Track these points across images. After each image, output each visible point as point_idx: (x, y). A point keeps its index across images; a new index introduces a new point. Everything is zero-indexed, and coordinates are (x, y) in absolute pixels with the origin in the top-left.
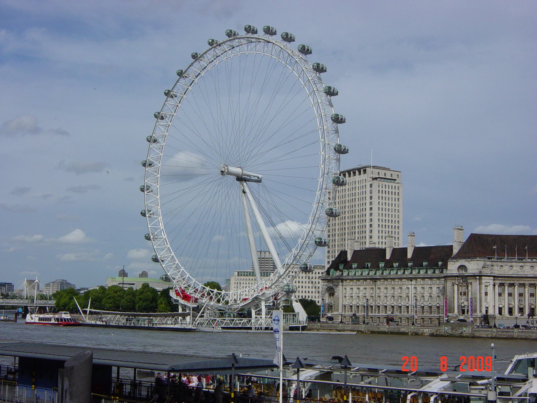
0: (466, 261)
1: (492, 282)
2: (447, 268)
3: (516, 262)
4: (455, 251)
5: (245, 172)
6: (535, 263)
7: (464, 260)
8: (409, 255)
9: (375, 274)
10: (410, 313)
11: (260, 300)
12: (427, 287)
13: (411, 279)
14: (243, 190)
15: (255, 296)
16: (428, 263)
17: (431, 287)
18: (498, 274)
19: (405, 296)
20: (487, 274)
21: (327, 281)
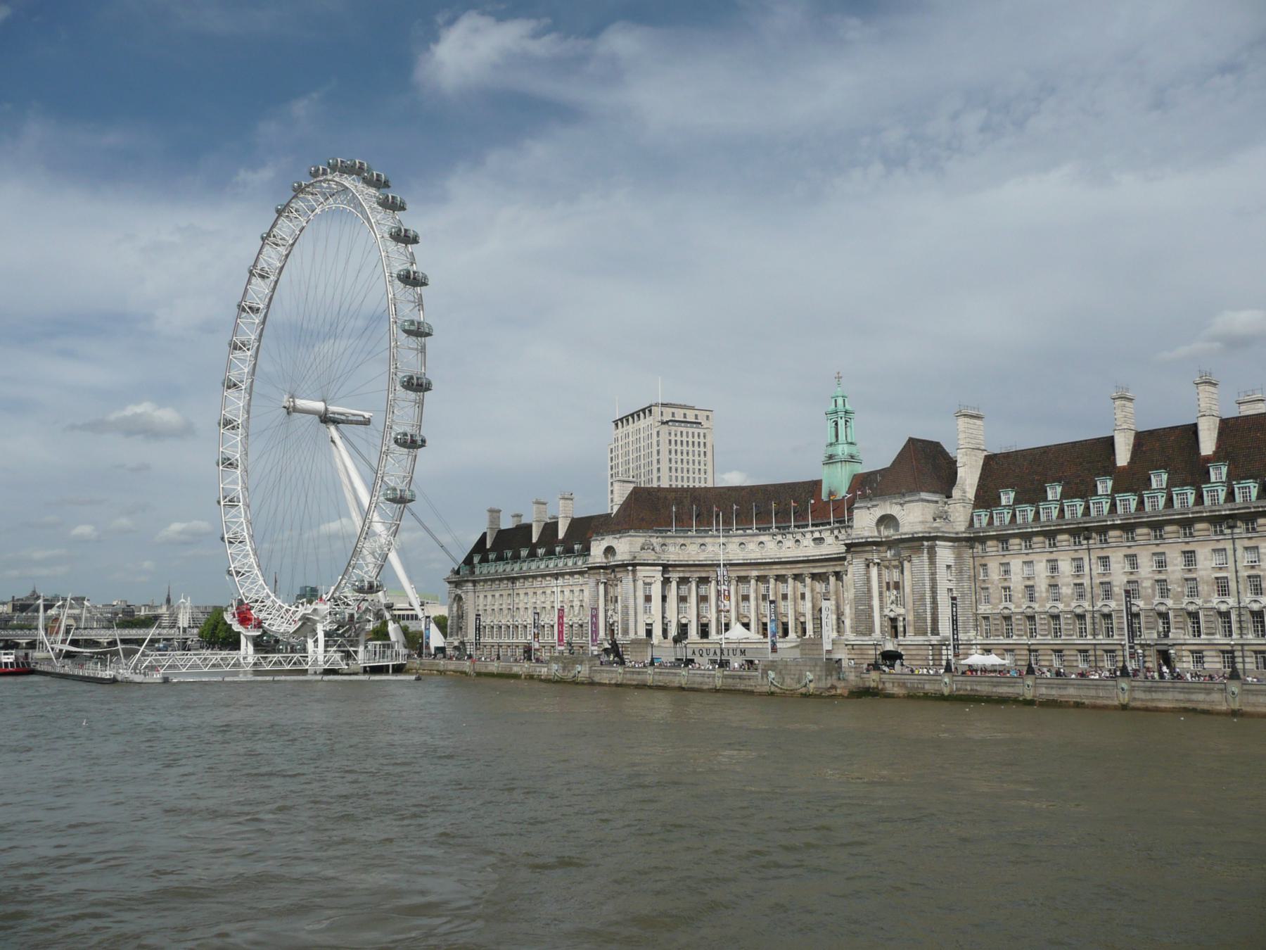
0: (615, 538)
1: (659, 577)
2: (589, 555)
3: (712, 536)
5: (332, 408)
6: (747, 538)
7: (611, 537)
8: (561, 535)
11: (315, 622)
13: (556, 576)
14: (331, 438)
16: (582, 547)
17: (582, 588)
18: (675, 561)
19: (549, 608)
20: (646, 562)
21: (453, 585)
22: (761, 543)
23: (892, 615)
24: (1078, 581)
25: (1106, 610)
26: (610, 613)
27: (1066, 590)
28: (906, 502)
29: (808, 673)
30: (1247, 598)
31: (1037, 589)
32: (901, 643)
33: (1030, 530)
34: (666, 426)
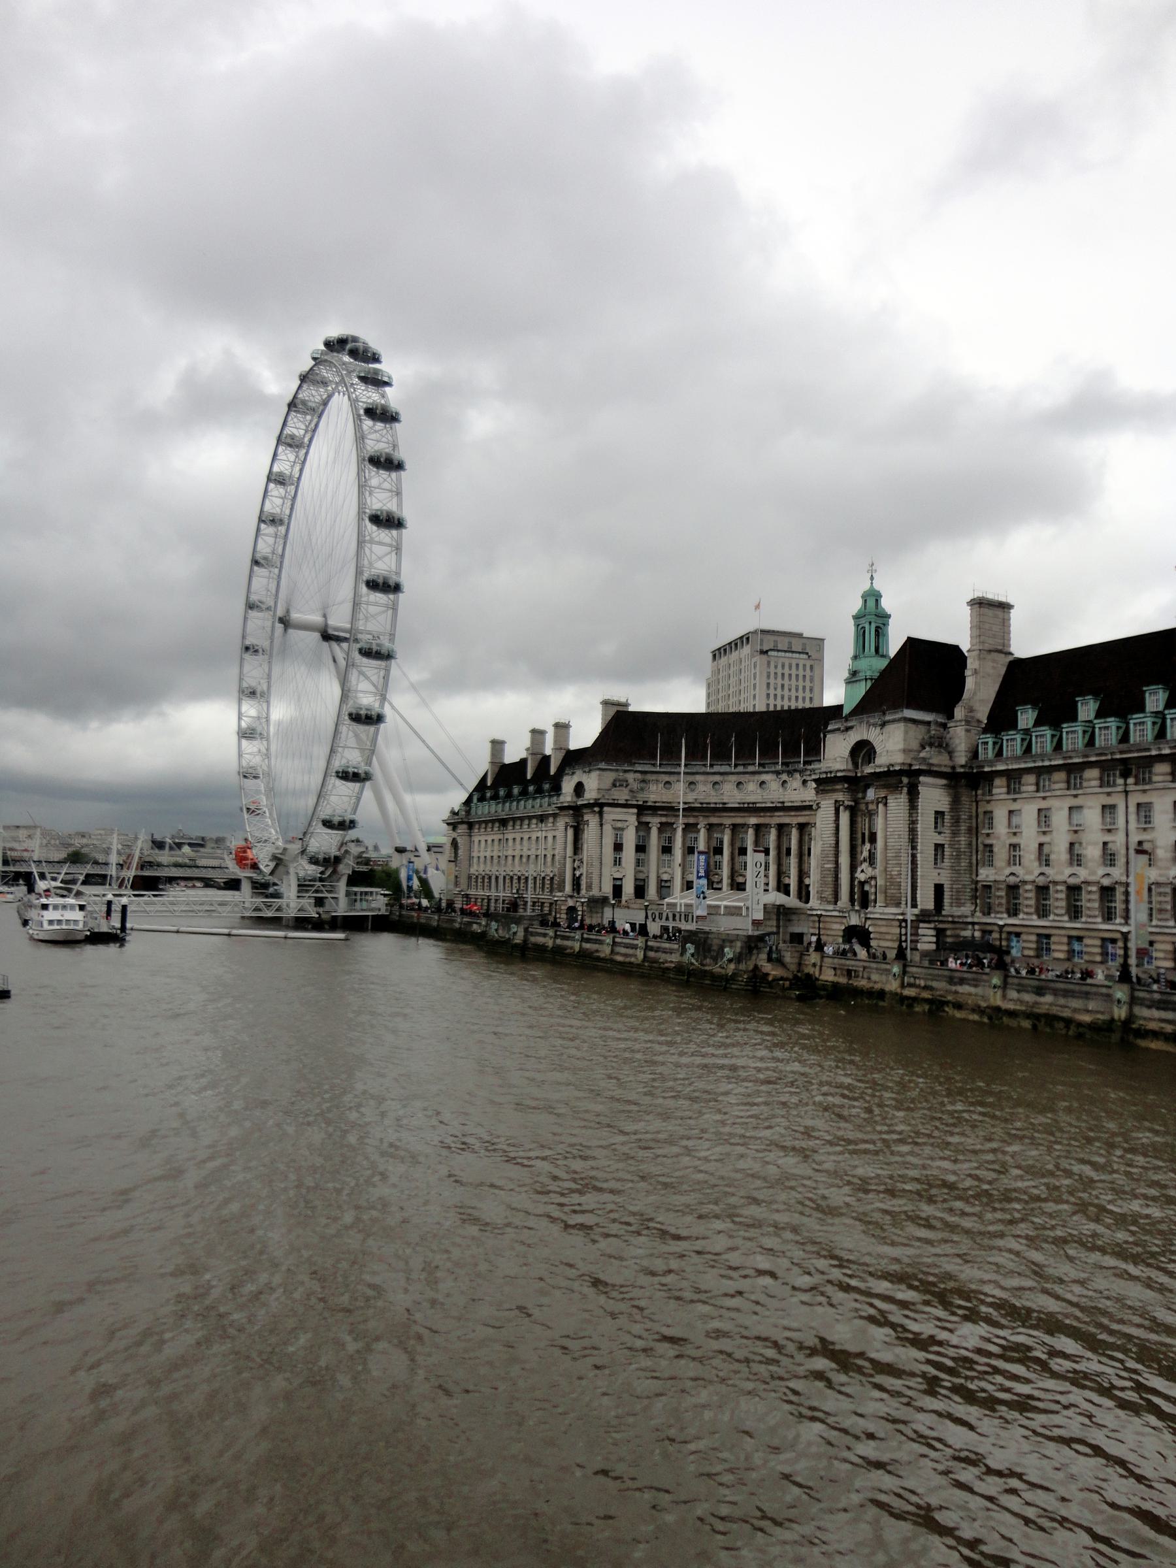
0: (585, 772)
8: (553, 771)
21: (451, 827)
22: (763, 783)
24: (1108, 838)
27: (1092, 852)
28: (889, 722)
31: (1055, 849)
32: (869, 916)
33: (1047, 763)
34: (764, 657)
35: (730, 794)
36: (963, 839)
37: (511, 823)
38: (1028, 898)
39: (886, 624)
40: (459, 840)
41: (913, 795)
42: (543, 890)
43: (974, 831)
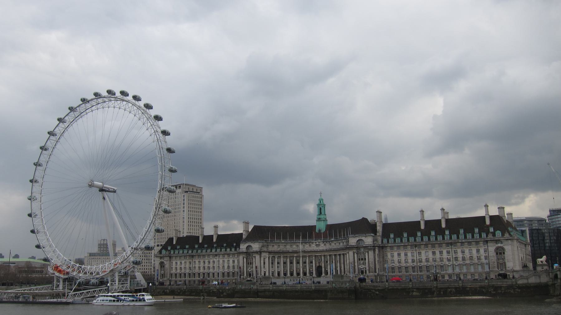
0: (252, 243)
1: (267, 255)
2: (239, 248)
4: (244, 237)
5: (105, 185)
8: (214, 240)
9: (192, 252)
10: (215, 277)
12: (226, 260)
14: (104, 197)
15: (111, 269)
17: (229, 259)
19: (212, 266)
21: (159, 258)
22: (298, 245)
23: (362, 267)
24: (413, 258)
25: (420, 266)
26: (249, 268)
27: (410, 261)
29: (347, 284)
30: (454, 262)
31: (401, 260)
34: (188, 194)
35: (289, 248)
36: (381, 259)
37: (197, 256)
38: (397, 270)
39: (324, 207)
40: (164, 262)
41: (374, 250)
42: (218, 277)
43: (383, 257)
